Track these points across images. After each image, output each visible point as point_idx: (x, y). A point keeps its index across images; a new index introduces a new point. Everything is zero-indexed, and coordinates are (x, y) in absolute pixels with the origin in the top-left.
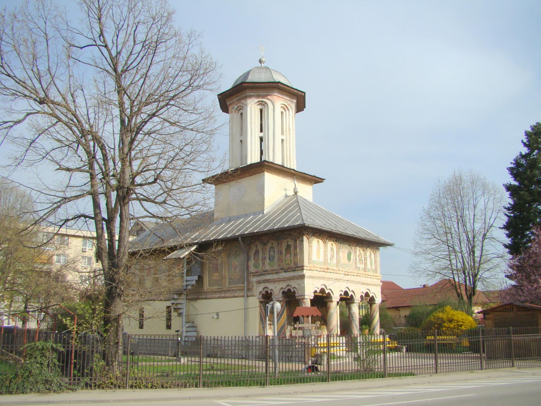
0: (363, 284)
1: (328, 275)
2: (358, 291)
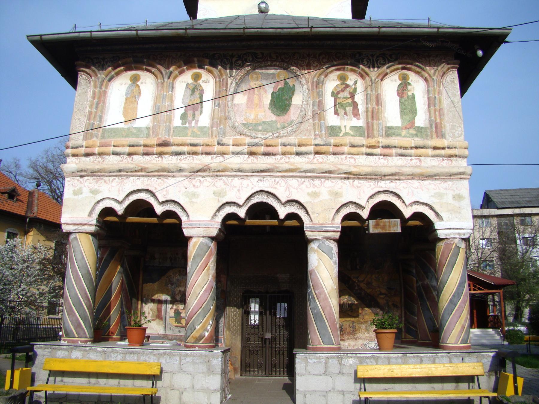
0: (357, 176)
1: (169, 161)
2: (322, 204)
